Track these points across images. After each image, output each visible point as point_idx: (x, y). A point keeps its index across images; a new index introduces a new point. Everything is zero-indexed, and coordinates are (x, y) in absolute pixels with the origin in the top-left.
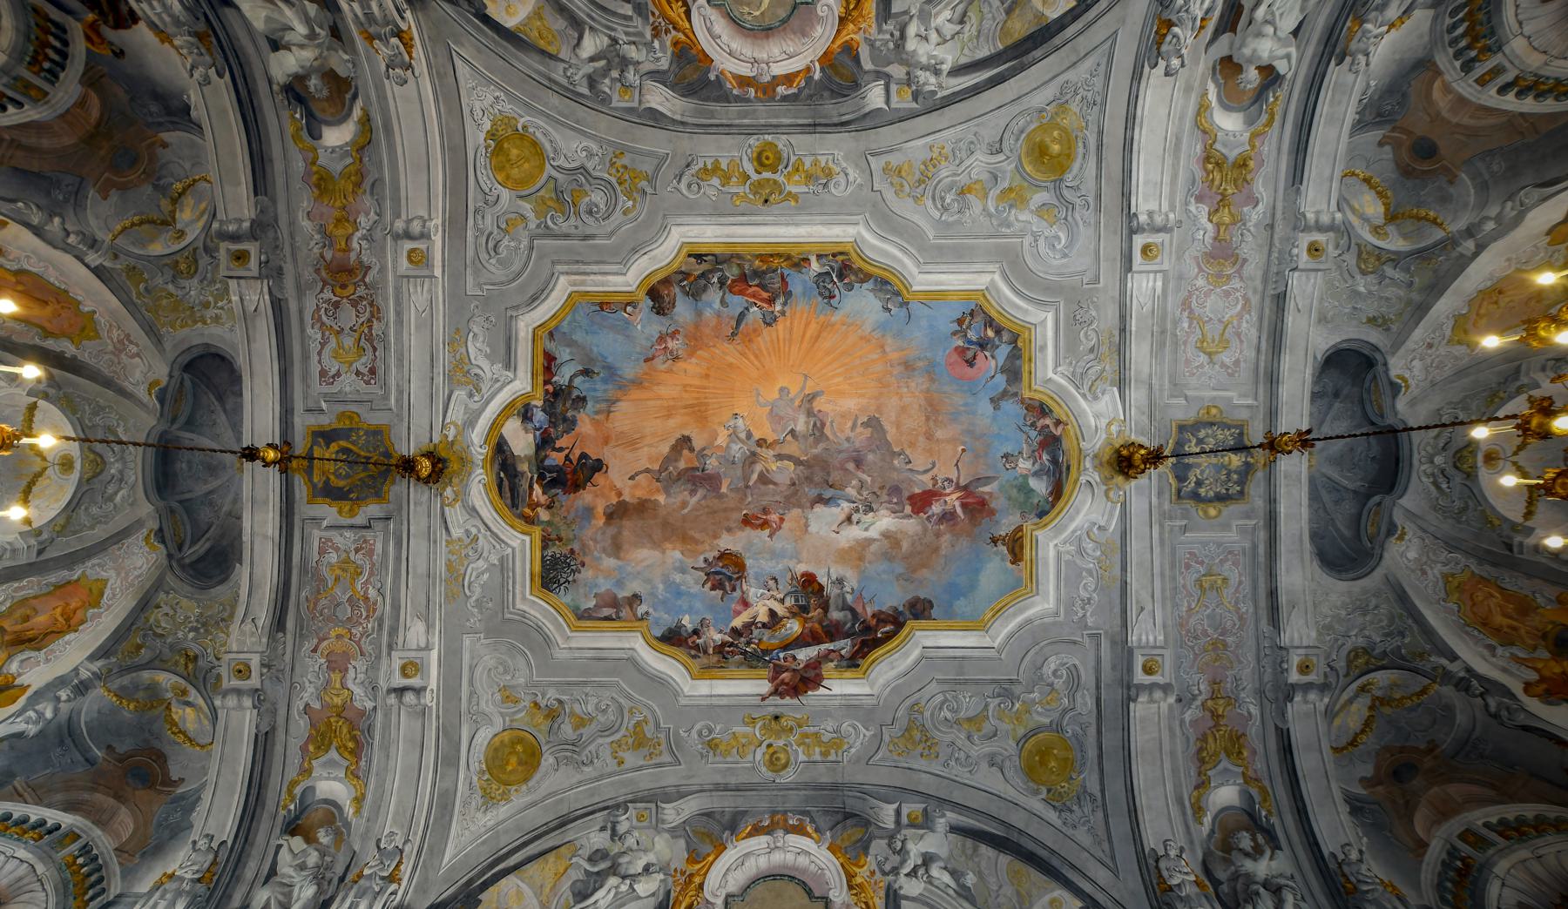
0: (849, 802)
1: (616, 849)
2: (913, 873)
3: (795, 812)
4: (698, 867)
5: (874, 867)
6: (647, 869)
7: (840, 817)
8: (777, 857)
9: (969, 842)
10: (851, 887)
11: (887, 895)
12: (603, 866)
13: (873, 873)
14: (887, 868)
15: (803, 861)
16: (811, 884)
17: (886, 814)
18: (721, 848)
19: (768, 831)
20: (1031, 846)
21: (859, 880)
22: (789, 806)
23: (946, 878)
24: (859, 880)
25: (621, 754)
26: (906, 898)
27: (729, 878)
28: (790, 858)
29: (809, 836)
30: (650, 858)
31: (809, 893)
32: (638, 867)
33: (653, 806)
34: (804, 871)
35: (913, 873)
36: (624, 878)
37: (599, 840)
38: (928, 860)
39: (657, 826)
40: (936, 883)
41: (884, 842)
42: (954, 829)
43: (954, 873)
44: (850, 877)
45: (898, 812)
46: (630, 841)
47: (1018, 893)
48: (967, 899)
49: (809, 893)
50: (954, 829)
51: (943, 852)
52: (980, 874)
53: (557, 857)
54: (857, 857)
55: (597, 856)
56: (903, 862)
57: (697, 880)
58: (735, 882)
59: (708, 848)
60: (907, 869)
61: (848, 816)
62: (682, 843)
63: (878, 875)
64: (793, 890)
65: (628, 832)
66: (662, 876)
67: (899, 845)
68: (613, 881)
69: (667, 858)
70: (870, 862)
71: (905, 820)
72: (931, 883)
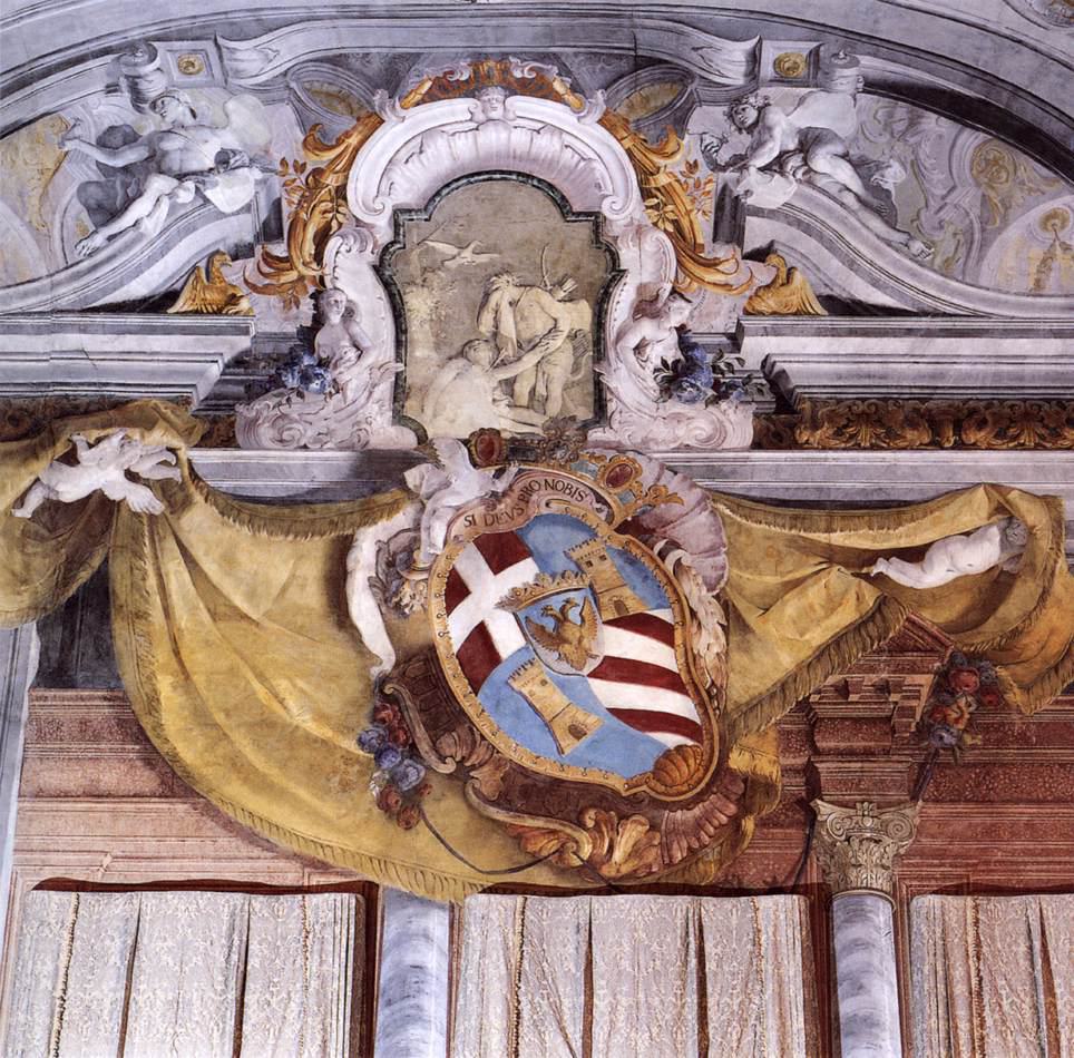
0: (642, 36)
1: (149, 125)
2: (778, 165)
3: (524, 56)
5: (696, 155)
6: (224, 160)
7: (624, 65)
8: (494, 140)
9: (902, 110)
10: (646, 194)
11: (719, 207)
13: (693, 167)
14: (724, 156)
15: (546, 145)
16: (566, 188)
17: (730, 61)
18: (374, 122)
19: (471, 89)
20: (1030, 113)
21: (662, 180)
22: (509, 44)
23: (845, 174)
24: (662, 180)
26: (758, 212)
27: (396, 175)
28: (519, 140)
29: (558, 98)
30: (227, 140)
31: (562, 204)
33: (209, 46)
34: (551, 164)
35: (778, 165)
37: (115, 110)
38: (808, 142)
39: (228, 82)
40: (821, 182)
41: (719, 112)
42: (872, 86)
43: (860, 165)
44: (645, 174)
45: (754, 58)
46: (176, 111)
47: (985, 199)
48: (878, 212)
49: (562, 204)
50: (872, 86)
51: (845, 128)
52: (915, 168)
53: (35, 140)
54: (661, 139)
55: (109, 140)
56: (758, 145)
58: (410, 185)
59: (342, 123)
61: (642, 62)
62: (287, 112)
63: (704, 171)
64: (527, 199)
65: (166, 94)
66: (257, 174)
67: (751, 115)
68: (158, 184)
69: (261, 140)
70: (689, 147)
71: (767, 70)
72: (810, 183)
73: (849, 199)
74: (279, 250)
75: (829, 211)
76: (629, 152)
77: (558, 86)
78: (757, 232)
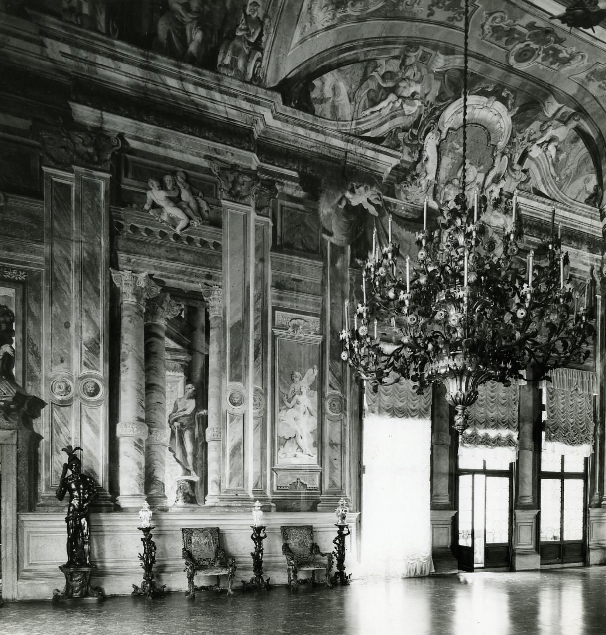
2: (540, 145)
4: (441, 104)
5: (526, 136)
12: (390, 84)
14: (532, 138)
21: (515, 140)
25: (435, 9)
32: (407, 93)
35: (540, 145)
36: (399, 97)
43: (558, 151)
44: (513, 136)
51: (561, 139)
56: (541, 137)
57: (437, 113)
60: (539, 142)
72: (545, 152)
73: (550, 160)
74: (415, 132)
75: (545, 164)
76: (513, 129)
77: (509, 103)
78: (527, 163)
